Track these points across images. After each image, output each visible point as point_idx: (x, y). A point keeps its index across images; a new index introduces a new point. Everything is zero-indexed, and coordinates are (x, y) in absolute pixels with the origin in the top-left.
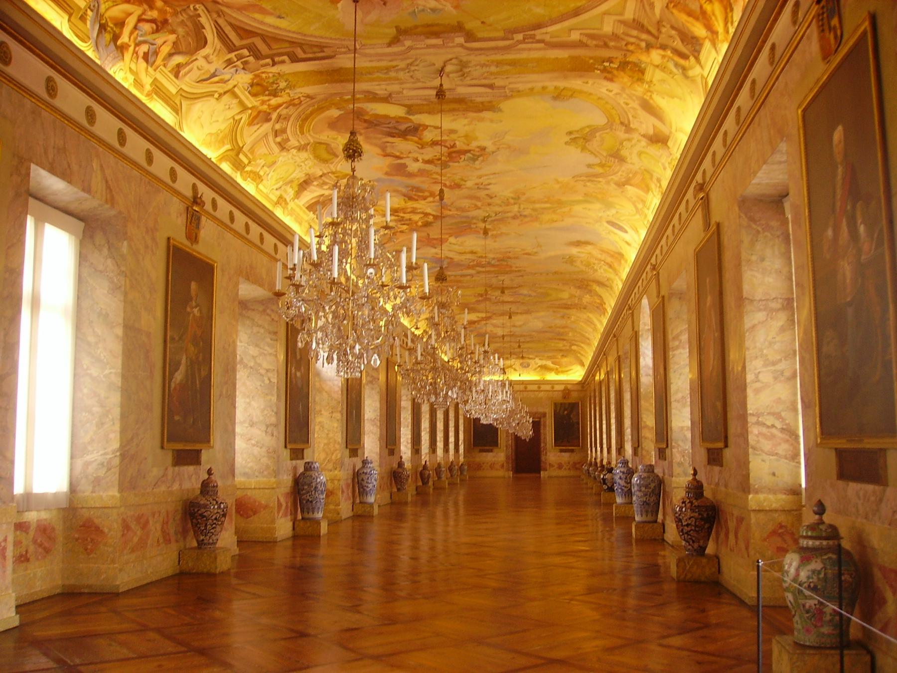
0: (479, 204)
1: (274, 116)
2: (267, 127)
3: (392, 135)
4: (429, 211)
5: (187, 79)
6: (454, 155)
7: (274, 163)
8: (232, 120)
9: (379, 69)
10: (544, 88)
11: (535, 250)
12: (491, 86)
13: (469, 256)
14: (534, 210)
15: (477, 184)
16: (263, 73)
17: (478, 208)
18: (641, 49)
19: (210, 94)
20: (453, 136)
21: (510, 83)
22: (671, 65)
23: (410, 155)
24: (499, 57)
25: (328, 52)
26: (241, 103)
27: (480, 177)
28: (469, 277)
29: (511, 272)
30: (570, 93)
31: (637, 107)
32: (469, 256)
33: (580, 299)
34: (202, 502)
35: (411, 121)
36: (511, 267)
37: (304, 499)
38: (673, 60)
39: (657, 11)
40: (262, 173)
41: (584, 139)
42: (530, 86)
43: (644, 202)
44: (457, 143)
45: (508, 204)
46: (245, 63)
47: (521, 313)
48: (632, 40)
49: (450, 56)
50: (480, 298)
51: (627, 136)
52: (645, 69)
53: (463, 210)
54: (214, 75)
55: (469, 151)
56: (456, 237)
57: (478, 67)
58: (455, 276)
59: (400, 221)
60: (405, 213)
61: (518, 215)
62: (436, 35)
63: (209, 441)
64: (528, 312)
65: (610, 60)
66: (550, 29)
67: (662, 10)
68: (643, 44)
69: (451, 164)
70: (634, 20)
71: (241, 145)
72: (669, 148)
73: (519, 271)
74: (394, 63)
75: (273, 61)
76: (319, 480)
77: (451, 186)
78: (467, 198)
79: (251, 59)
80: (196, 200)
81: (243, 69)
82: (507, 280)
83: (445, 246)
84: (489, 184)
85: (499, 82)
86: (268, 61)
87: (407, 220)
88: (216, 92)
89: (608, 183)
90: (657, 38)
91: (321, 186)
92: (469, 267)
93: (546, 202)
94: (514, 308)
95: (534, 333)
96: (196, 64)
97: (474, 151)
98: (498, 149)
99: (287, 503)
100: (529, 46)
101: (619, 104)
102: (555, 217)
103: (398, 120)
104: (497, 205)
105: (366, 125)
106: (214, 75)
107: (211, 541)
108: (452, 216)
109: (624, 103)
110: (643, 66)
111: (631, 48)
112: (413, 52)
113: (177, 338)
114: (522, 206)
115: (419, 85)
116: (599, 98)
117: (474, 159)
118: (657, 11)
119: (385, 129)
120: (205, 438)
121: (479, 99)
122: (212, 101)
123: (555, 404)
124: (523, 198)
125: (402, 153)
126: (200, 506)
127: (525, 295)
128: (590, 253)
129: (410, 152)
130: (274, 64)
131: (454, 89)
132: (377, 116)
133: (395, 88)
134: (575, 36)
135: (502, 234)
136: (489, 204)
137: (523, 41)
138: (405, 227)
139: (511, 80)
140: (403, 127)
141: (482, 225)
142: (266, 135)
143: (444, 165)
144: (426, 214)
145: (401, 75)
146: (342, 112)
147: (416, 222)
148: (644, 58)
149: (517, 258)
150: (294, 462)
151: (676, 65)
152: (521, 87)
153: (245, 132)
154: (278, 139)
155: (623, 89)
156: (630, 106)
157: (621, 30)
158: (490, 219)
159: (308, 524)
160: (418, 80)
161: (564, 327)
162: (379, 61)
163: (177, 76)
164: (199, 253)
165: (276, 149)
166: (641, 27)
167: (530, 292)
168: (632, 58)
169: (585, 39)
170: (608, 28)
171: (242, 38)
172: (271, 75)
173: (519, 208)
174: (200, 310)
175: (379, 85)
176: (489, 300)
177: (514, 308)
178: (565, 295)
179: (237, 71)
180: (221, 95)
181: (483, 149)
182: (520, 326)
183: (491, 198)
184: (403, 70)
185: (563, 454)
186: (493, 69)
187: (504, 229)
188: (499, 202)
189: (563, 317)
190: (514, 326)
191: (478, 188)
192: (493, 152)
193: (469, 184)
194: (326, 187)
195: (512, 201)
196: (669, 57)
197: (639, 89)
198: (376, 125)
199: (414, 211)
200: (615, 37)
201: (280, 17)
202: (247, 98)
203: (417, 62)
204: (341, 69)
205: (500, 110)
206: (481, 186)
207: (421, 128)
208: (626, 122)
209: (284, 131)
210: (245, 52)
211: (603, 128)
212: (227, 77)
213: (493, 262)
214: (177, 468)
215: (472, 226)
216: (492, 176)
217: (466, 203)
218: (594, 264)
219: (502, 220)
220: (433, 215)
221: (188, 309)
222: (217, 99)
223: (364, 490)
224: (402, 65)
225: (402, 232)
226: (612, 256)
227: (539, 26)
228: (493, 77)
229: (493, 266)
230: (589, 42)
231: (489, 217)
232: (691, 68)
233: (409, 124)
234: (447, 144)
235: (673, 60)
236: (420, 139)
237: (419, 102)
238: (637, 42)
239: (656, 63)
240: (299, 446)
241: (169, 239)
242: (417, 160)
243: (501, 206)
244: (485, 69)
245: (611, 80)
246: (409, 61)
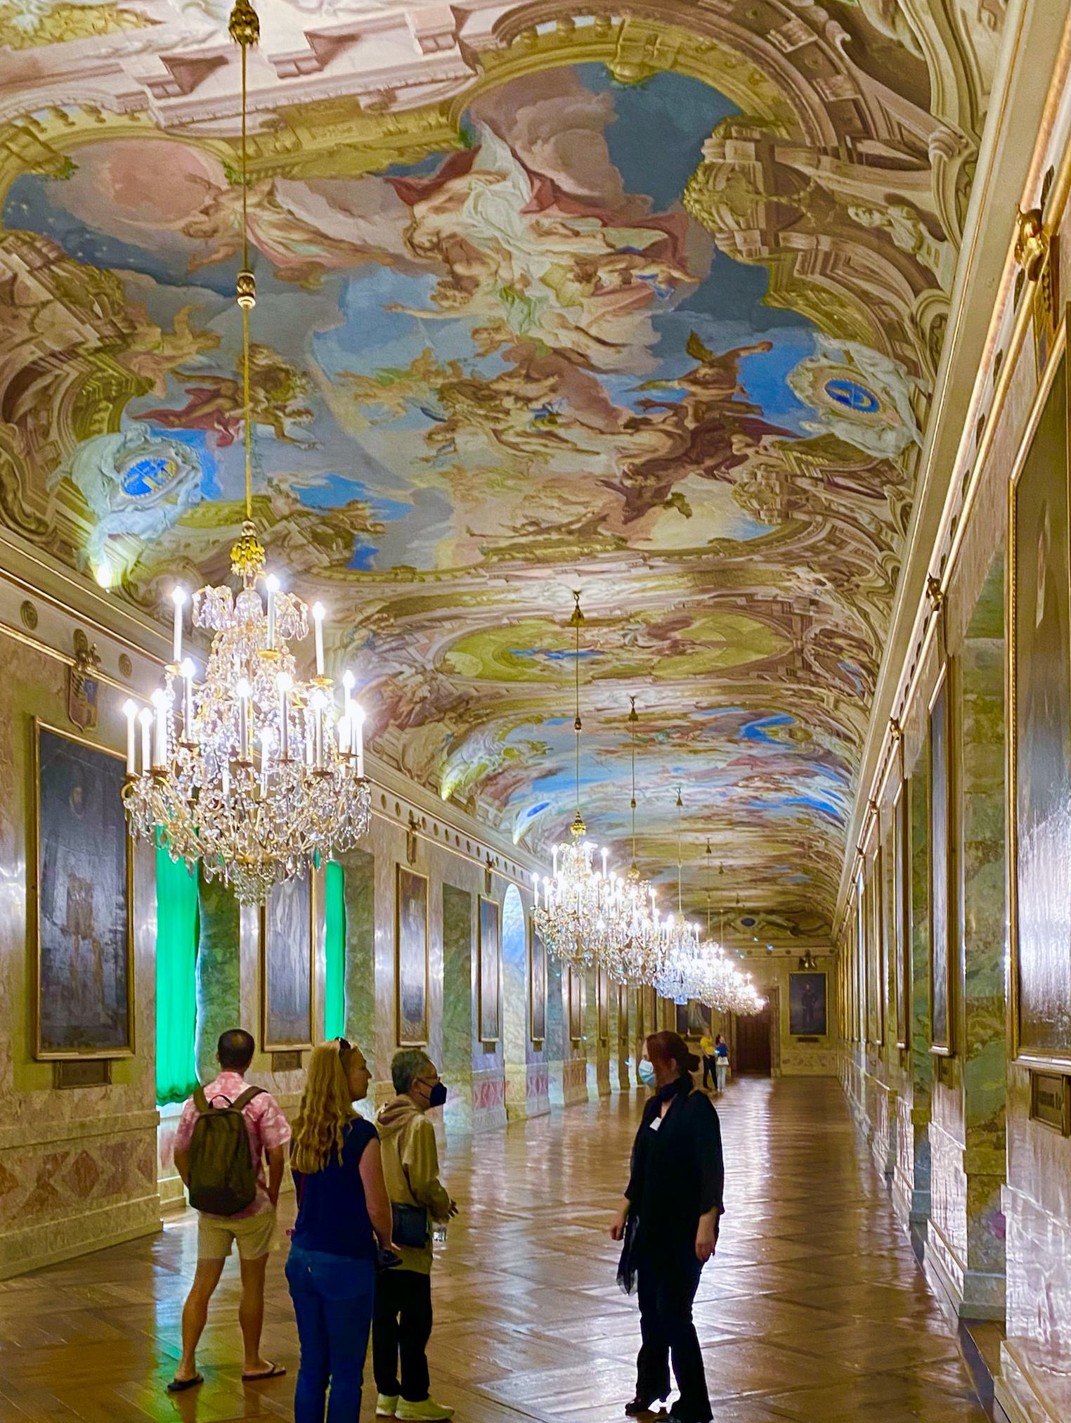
11: (603, 758)
13: (700, 746)
28: (704, 705)
50: (677, 635)
108: (716, 787)
149: (625, 745)
199: (758, 789)
229: (659, 730)
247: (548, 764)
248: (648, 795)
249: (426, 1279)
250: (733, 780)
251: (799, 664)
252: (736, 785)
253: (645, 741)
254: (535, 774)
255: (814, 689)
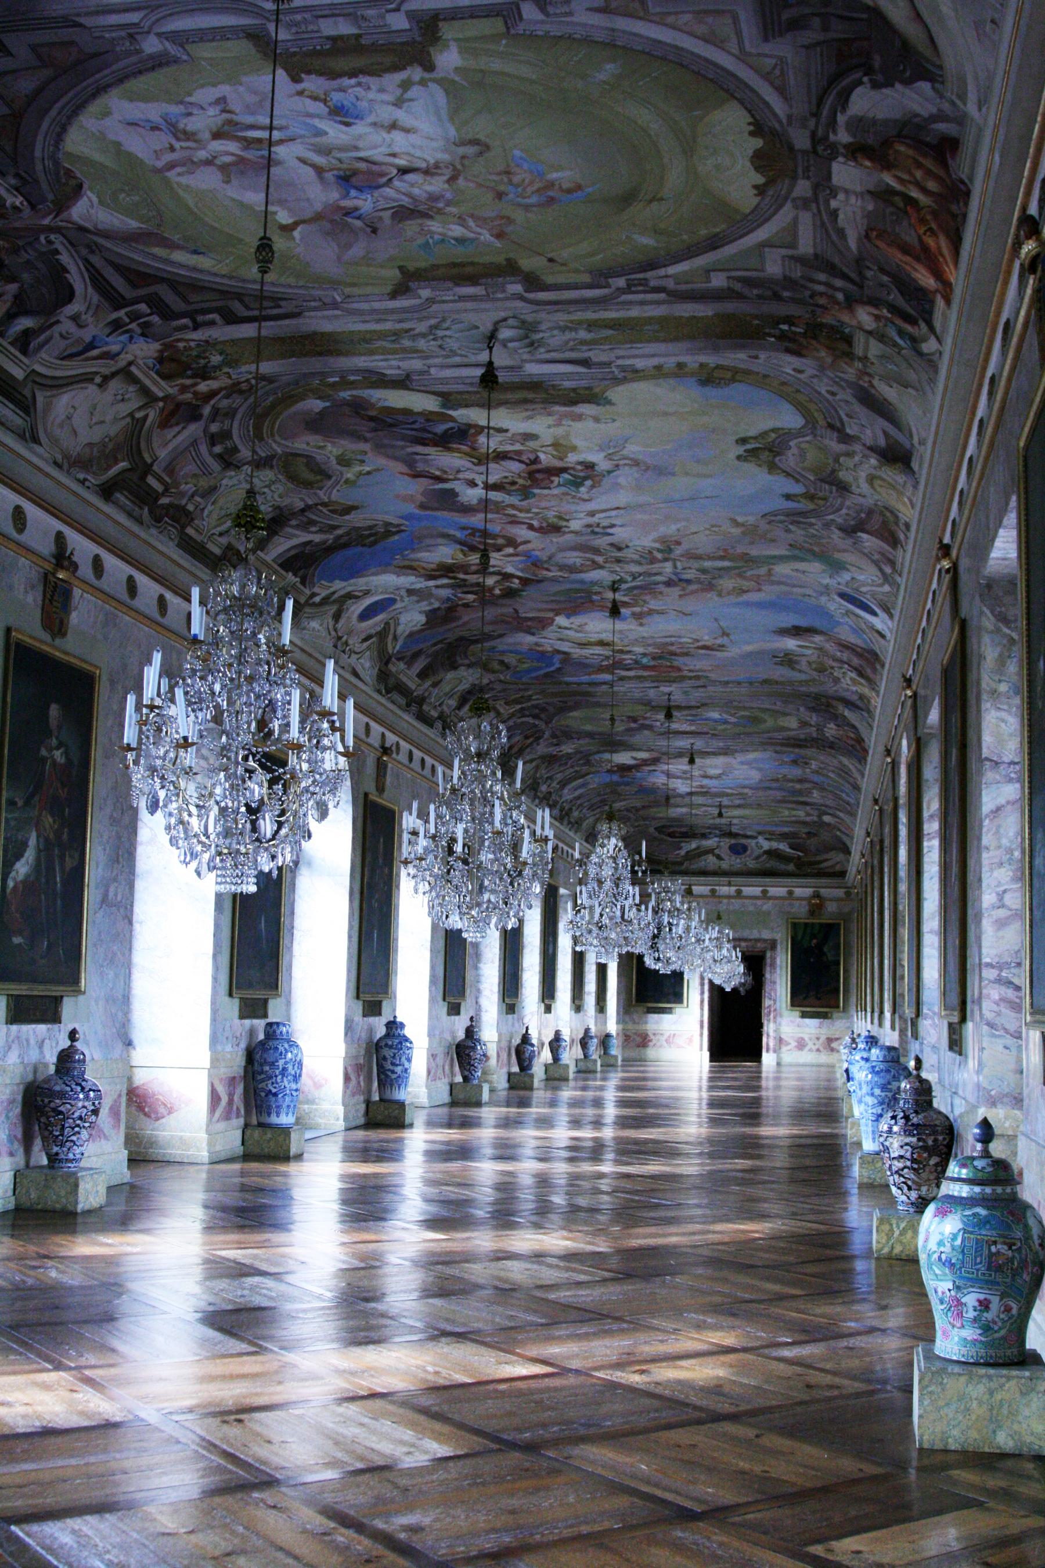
0: (600, 559)
1: (207, 411)
2: (194, 429)
3: (423, 443)
4: (510, 569)
5: (43, 354)
6: (539, 476)
7: (214, 489)
8: (128, 420)
9: (382, 335)
10: (680, 366)
11: (719, 641)
12: (585, 363)
14: (704, 571)
15: (588, 526)
16: (179, 340)
17: (597, 566)
18: (838, 303)
19: (86, 379)
20: (532, 444)
21: (618, 358)
22: (893, 333)
23: (461, 476)
24: (590, 315)
25: (287, 307)
26: (145, 391)
27: (592, 514)
29: (683, 679)
30: (729, 375)
31: (851, 399)
32: (598, 650)
33: (820, 729)
34: (57, 1088)
35: (452, 419)
36: (679, 670)
37: (263, 1090)
38: (893, 323)
39: (853, 244)
40: (191, 507)
41: (770, 451)
42: (655, 361)
43: (892, 563)
44: (542, 456)
45: (653, 561)
46: (146, 326)
47: (714, 754)
48: (821, 288)
49: (503, 314)
50: (633, 725)
51: (842, 447)
52: (852, 337)
53: (572, 569)
54: (91, 346)
55: (564, 470)
56: (568, 617)
57: (555, 332)
58: (579, 684)
59: (460, 586)
60: (466, 573)
61: (674, 577)
62: (472, 280)
63: (76, 981)
64: (725, 752)
65: (789, 320)
66: (671, 270)
67: (859, 240)
68: (840, 296)
69: (536, 491)
70: (816, 255)
71: (149, 461)
72: (914, 472)
73: (697, 678)
74: (406, 326)
75: (194, 321)
76: (289, 1055)
77: (541, 528)
78: (574, 548)
79: (155, 319)
80: (62, 557)
81: (143, 335)
82: (676, 692)
83: (550, 632)
84: (613, 526)
85: (597, 355)
86: (185, 321)
87: (472, 585)
88: (96, 373)
89: (827, 525)
90: (861, 287)
91: (305, 526)
92: (601, 669)
93: (722, 558)
94: (699, 744)
95: (746, 791)
96: (57, 329)
97: (573, 469)
98: (617, 466)
99: (231, 1096)
100: (641, 296)
101: (819, 393)
102: (746, 584)
103: (429, 417)
104: (632, 561)
105: (373, 424)
106: (91, 346)
107: (71, 1156)
108: (553, 580)
109: (828, 392)
110: (847, 331)
111: (822, 301)
112: (435, 307)
113: (20, 803)
114: (679, 564)
115: (457, 360)
116: (784, 384)
117: (577, 483)
118: (853, 244)
119: (409, 432)
120: (72, 979)
121: (567, 384)
122: (92, 388)
123: (795, 925)
124: (678, 551)
125: (445, 472)
126: (53, 1094)
127: (716, 721)
128: (820, 649)
129: (459, 471)
130: (196, 327)
131: (520, 367)
132: (390, 411)
133: (416, 364)
134: (718, 281)
135: (651, 612)
136: (618, 561)
137: (629, 289)
138: (471, 597)
139: (621, 353)
140: (440, 428)
141: (610, 595)
142: (194, 443)
143: (525, 493)
144: (507, 577)
145: (422, 344)
146: (328, 404)
147: (491, 589)
148: (846, 318)
149: (687, 654)
150: (247, 1022)
151: (901, 333)
152: (639, 363)
153: (155, 439)
154: (218, 449)
155: (822, 368)
156: (838, 397)
157: (797, 273)
158: (624, 586)
159: (269, 1135)
160: (454, 353)
161: (801, 781)
162: (378, 321)
163: (25, 352)
164: (66, 653)
165: (215, 466)
166: (832, 269)
167: (725, 716)
168: (828, 319)
169: (737, 287)
170: (774, 267)
171: (134, 286)
172: (192, 344)
173: (675, 567)
174: (66, 753)
175: (386, 360)
176: (650, 728)
177: (699, 744)
178: (792, 722)
179: (131, 338)
180: (106, 379)
181: (590, 466)
182: (718, 777)
183: (620, 549)
184: (424, 335)
185: (807, 1021)
186: (582, 334)
187: (654, 604)
188: (636, 557)
189: (795, 762)
190: (706, 777)
191: (593, 533)
192: (609, 472)
193: (575, 525)
194: (313, 529)
195: (659, 556)
196: (886, 319)
197: (850, 372)
198: (391, 425)
200: (788, 282)
201: (196, 252)
202: (155, 383)
203: (445, 325)
204: (315, 333)
205: (609, 402)
206: (597, 530)
207: (472, 431)
208: (838, 424)
209: (226, 435)
210: (143, 307)
211: (800, 433)
212: (115, 348)
213: (645, 661)
214: (14, 1028)
215: (595, 597)
216: (613, 513)
217: (574, 558)
218: (832, 668)
219: (649, 588)
220: (518, 577)
221: (44, 752)
222: (100, 386)
223: (387, 1076)
224: (422, 327)
225: (466, 606)
226: (860, 655)
227: (652, 265)
228: (585, 348)
229: (645, 668)
230: (746, 291)
231: (622, 581)
232: (925, 340)
233: (451, 425)
234: (524, 458)
235: (893, 323)
236: (474, 449)
237: (461, 388)
238: (830, 292)
239: (869, 328)
240: (259, 995)
241: (8, 630)
242: (473, 484)
243: (640, 564)
244: (569, 335)
245: (798, 354)
246: (433, 322)
247: (791, 644)
248: (668, 567)
249: (713, 1058)
250: (531, 591)
251: (543, 716)
252: (525, 582)
253: (660, 658)
254: (818, 639)
255: (519, 707)
